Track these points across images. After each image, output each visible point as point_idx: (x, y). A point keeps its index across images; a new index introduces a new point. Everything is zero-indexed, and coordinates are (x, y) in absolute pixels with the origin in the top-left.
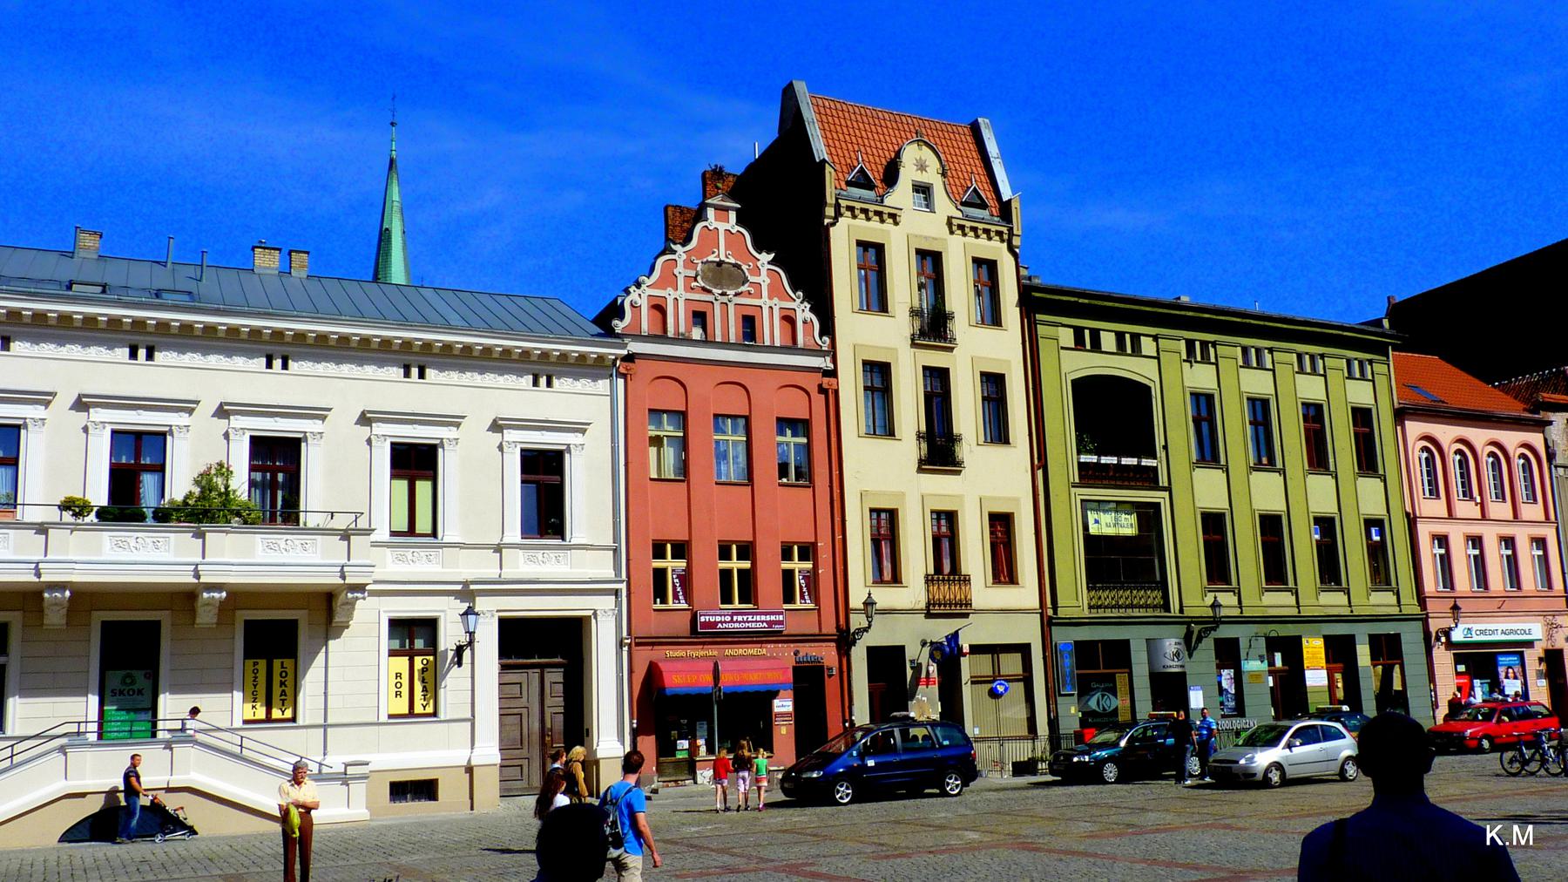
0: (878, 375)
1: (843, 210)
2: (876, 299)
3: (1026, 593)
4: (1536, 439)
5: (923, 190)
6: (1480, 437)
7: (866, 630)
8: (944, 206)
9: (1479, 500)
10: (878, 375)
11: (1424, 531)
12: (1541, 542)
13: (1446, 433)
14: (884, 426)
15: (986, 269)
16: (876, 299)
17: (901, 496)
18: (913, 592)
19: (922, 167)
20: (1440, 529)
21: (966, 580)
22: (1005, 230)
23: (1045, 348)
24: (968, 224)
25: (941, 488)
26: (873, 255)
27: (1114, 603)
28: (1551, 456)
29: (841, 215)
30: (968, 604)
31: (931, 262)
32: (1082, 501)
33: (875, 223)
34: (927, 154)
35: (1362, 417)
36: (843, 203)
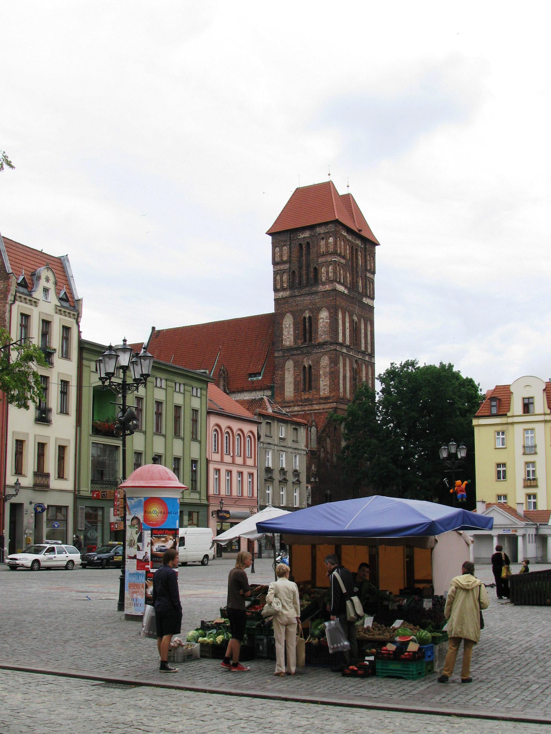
1: (17, 298)
3: (68, 484)
4: (254, 429)
5: (46, 290)
6: (236, 426)
7: (14, 495)
9: (232, 455)
11: (212, 467)
12: (251, 475)
13: (224, 423)
17: (28, 434)
18: (27, 480)
19: (47, 280)
20: (218, 466)
21: (48, 475)
22: (76, 313)
23: (85, 371)
24: (63, 310)
27: (97, 490)
28: (259, 438)
29: (16, 300)
30: (48, 486)
32: (92, 443)
33: (28, 306)
34: (50, 275)
35: (195, 411)
36: (18, 295)
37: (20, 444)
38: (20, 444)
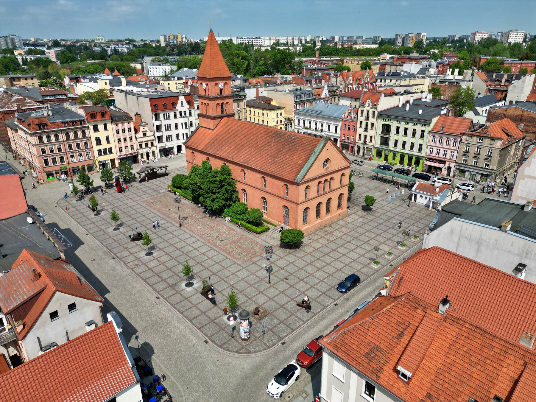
0: (361, 122)
2: (362, 115)
8: (371, 106)
10: (361, 122)
14: (361, 127)
15: (374, 112)
16: (362, 115)
18: (361, 142)
25: (365, 133)
26: (362, 111)
31: (368, 112)
37: (360, 135)
38: (360, 135)
